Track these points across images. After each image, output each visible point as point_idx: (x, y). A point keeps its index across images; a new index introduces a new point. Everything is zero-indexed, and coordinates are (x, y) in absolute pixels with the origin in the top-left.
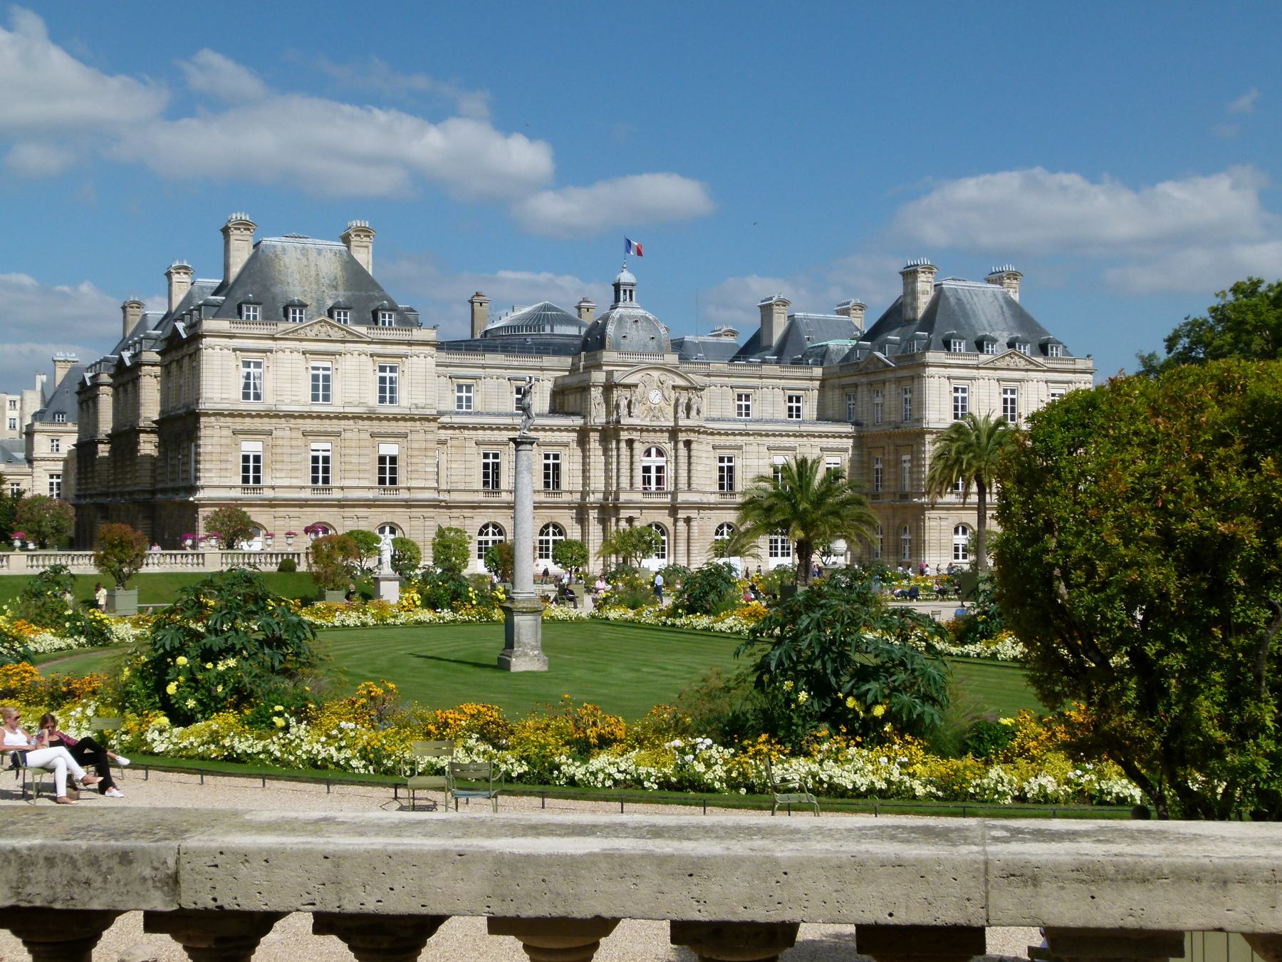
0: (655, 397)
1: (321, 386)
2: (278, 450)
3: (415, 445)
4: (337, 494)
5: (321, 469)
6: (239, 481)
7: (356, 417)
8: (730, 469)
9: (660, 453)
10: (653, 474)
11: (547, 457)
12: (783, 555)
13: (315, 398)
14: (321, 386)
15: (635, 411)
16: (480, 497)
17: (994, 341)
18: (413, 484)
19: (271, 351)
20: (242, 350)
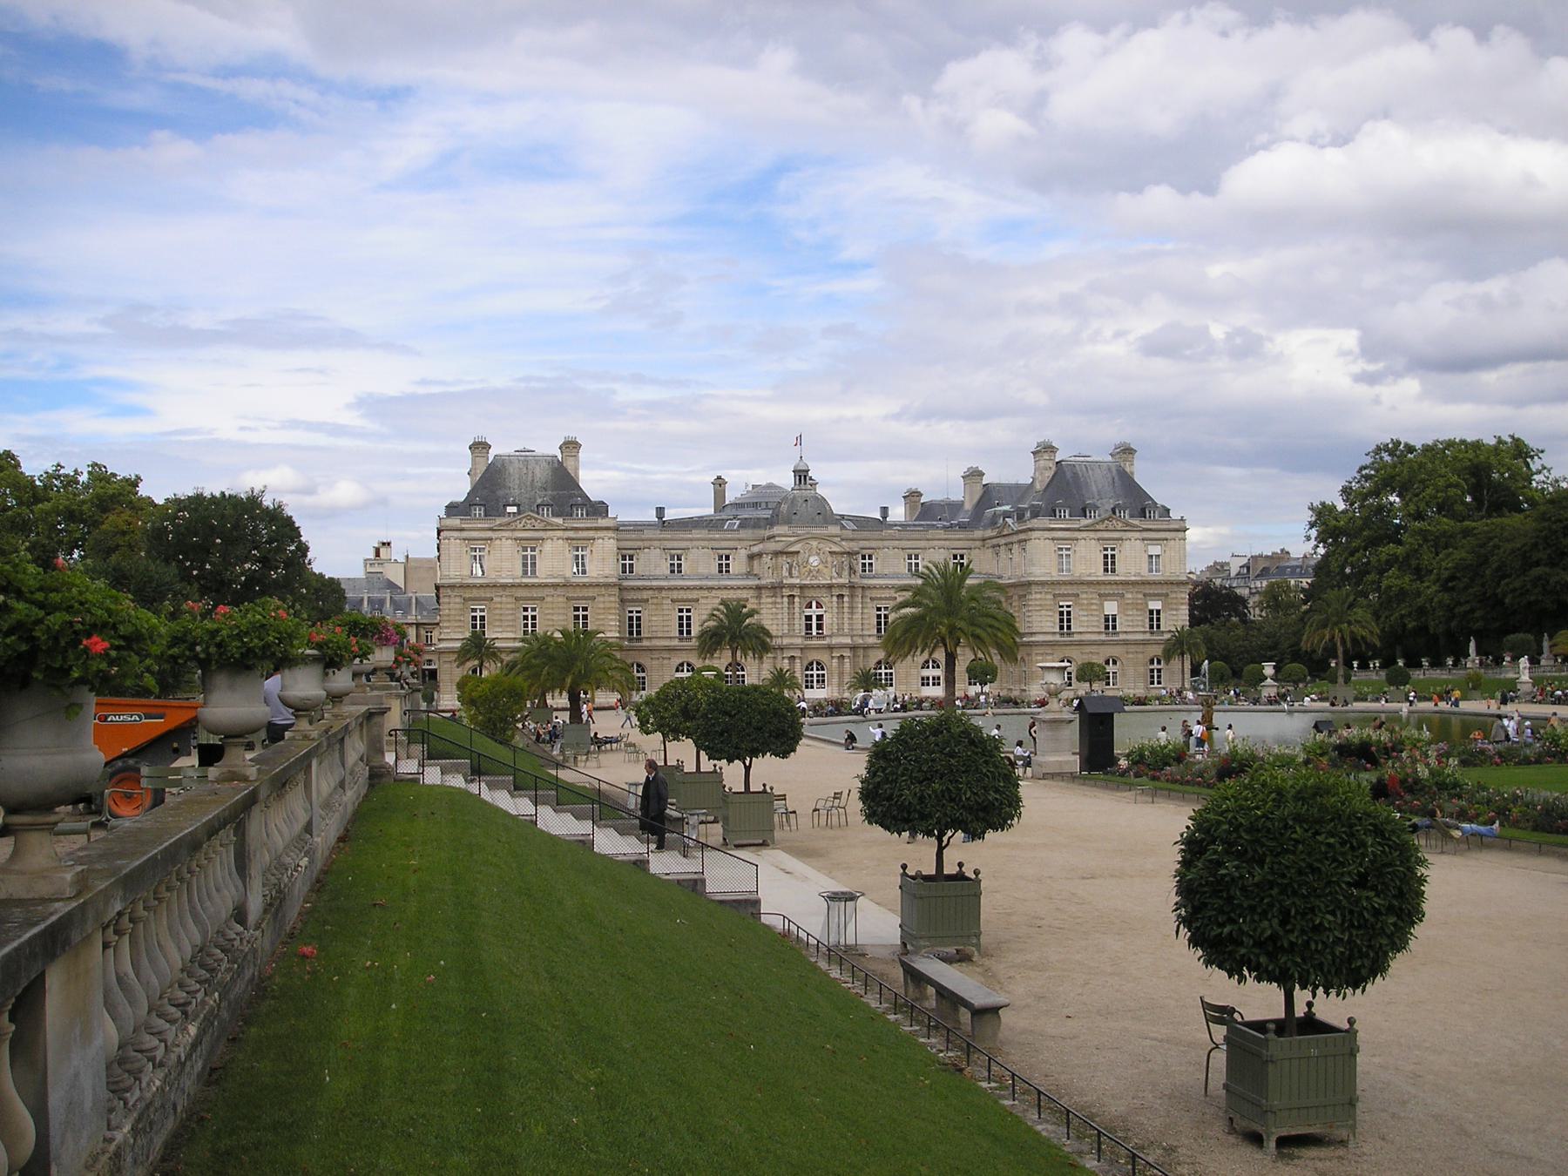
0: (814, 561)
1: (529, 565)
7: (555, 586)
9: (819, 606)
13: (525, 572)
14: (529, 565)
15: (795, 573)
16: (676, 643)
17: (1096, 508)
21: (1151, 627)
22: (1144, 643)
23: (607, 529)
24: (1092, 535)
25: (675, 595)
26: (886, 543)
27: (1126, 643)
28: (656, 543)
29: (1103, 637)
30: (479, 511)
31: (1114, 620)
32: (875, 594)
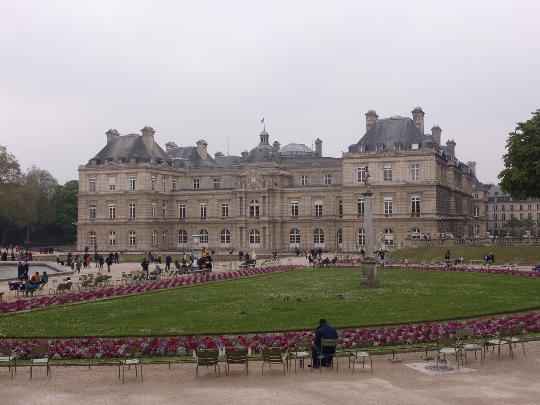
0: (254, 180)
2: (99, 207)
3: (140, 203)
4: (115, 221)
5: (113, 212)
6: (89, 217)
7: (121, 195)
8: (296, 207)
9: (257, 202)
10: (255, 210)
11: (224, 205)
12: (321, 242)
13: (111, 189)
15: (243, 186)
16: (199, 220)
18: (139, 217)
19: (97, 175)
20: (88, 175)
21: (414, 211)
22: (407, 220)
23: (142, 168)
24: (376, 160)
25: (199, 198)
26: (313, 169)
27: (396, 220)
28: (208, 174)
29: (383, 217)
30: (94, 163)
31: (391, 207)
32: (290, 195)
